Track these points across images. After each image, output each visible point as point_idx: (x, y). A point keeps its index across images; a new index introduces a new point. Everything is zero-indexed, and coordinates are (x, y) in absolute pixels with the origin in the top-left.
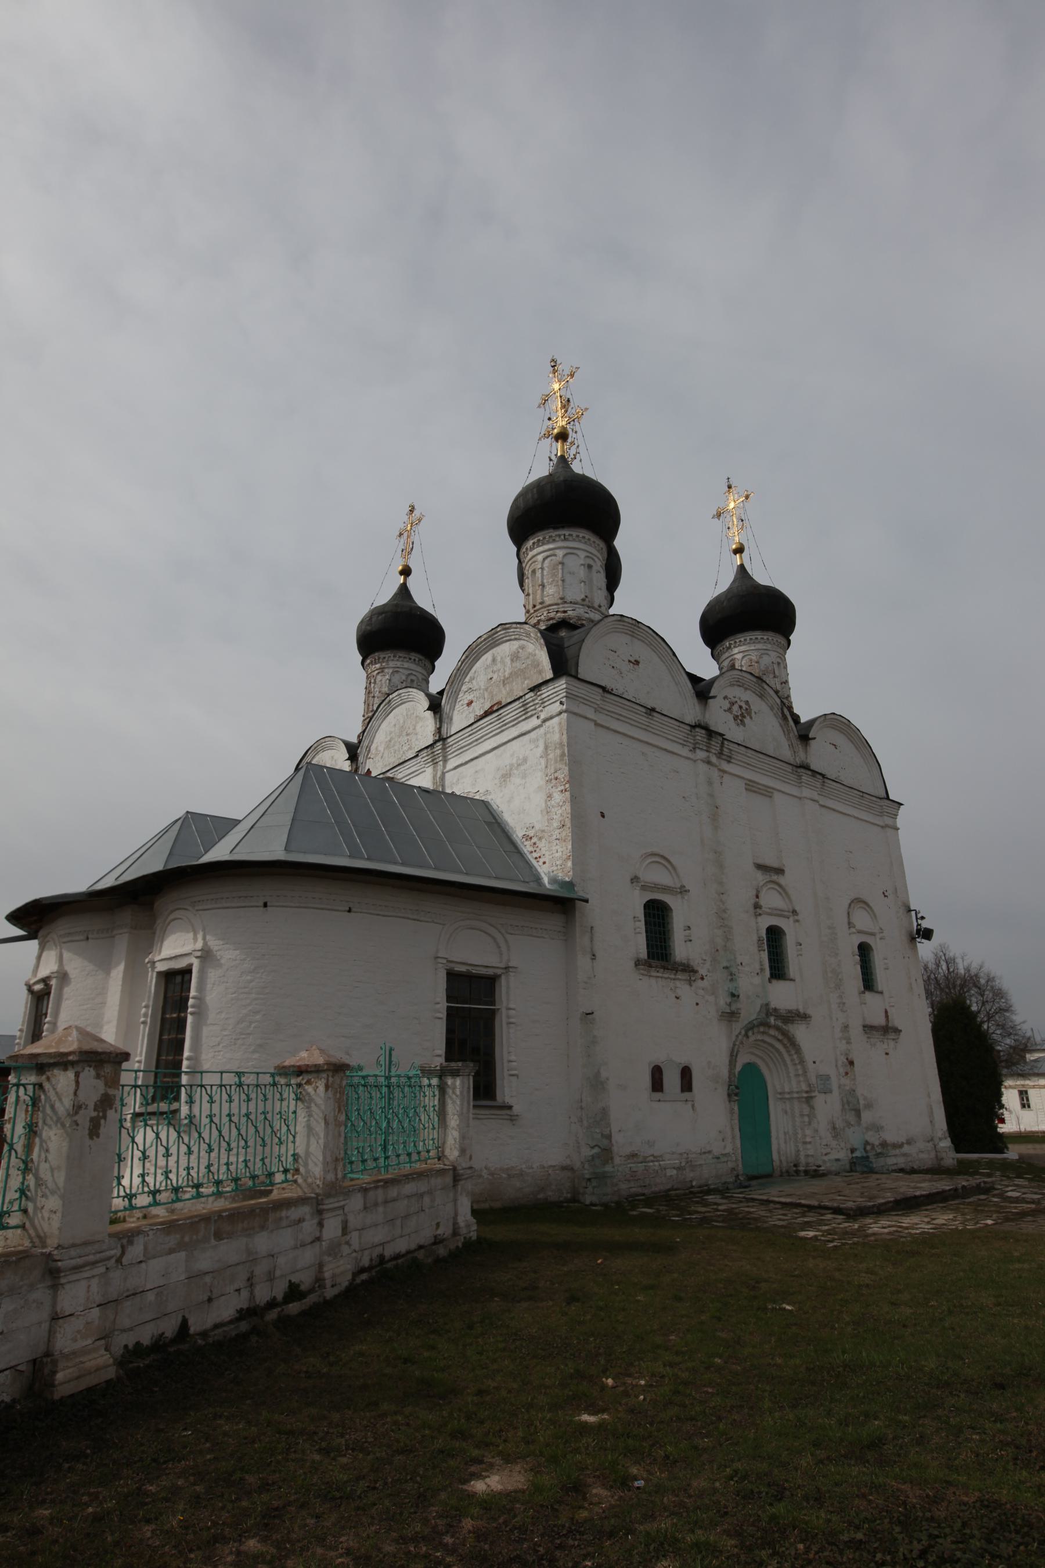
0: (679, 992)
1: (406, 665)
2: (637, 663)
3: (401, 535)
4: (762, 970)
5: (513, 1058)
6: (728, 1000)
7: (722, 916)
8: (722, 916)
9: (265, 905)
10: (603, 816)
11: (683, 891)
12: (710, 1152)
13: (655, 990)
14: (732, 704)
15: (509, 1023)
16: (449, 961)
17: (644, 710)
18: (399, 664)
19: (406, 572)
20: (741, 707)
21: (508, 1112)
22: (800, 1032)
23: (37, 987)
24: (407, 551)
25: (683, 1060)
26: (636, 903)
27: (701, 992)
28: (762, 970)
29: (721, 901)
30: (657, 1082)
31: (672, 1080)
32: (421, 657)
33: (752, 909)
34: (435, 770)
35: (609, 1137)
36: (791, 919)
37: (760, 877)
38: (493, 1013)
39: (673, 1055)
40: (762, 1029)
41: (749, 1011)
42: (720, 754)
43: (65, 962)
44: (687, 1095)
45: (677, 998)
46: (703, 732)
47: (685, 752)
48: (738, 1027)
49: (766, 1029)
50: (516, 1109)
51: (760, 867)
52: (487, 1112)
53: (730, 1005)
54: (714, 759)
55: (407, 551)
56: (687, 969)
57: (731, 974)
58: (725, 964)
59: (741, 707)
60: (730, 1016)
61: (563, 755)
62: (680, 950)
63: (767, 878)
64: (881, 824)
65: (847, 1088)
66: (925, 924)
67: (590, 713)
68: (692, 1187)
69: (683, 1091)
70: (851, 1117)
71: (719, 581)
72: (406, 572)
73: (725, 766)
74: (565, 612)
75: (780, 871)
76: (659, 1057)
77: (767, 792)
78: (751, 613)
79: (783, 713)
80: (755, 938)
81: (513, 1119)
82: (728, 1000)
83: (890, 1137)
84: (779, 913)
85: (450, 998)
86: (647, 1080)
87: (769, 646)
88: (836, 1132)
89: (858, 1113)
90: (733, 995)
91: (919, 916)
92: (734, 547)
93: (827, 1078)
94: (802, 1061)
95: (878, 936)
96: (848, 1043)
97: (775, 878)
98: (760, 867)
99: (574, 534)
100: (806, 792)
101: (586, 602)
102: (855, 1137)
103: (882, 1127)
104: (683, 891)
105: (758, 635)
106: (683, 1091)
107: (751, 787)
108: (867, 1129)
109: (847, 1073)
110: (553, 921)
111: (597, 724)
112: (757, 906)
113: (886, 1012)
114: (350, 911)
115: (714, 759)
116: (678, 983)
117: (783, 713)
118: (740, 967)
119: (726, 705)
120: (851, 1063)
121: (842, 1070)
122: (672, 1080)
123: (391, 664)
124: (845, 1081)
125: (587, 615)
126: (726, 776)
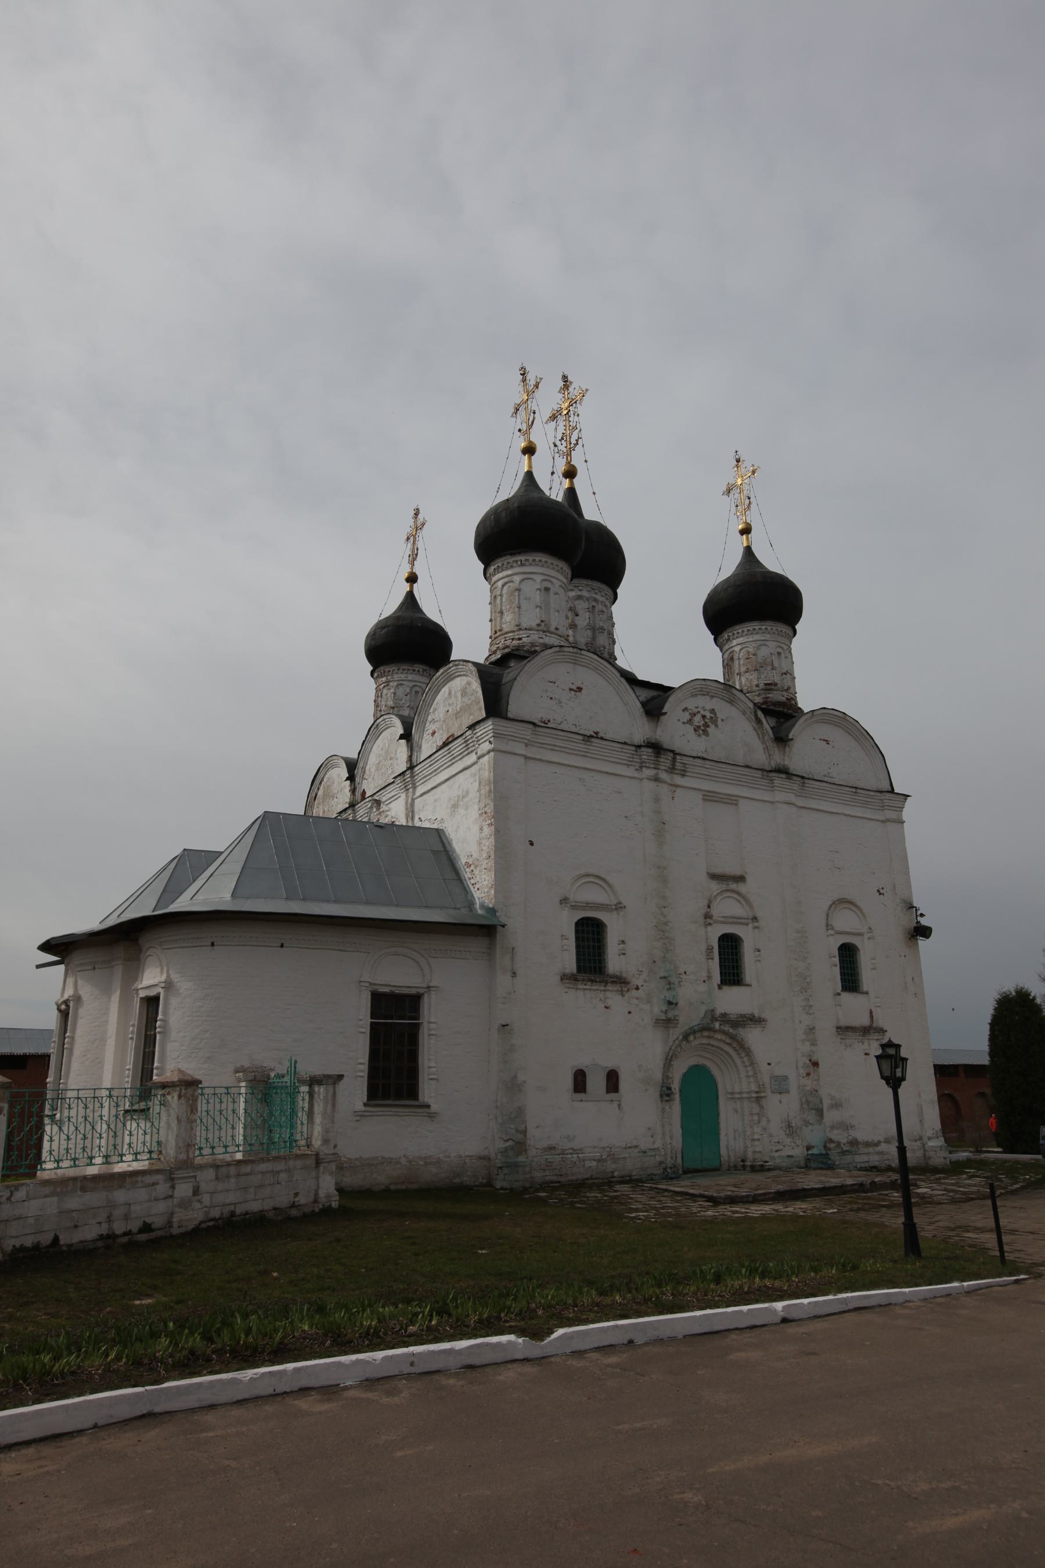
0: (609, 1002)
1: (410, 677)
2: (580, 689)
3: (408, 539)
4: (709, 977)
5: (433, 1064)
6: (664, 1008)
7: (663, 930)
8: (663, 930)
9: (213, 944)
10: (532, 844)
11: (619, 907)
12: (636, 1147)
13: (585, 1003)
15: (429, 1035)
16: (371, 984)
17: (581, 738)
18: (403, 676)
19: (412, 579)
20: (704, 717)
21: (426, 1110)
22: (752, 1036)
23: (63, 1007)
24: (413, 557)
25: (611, 1064)
26: (566, 923)
27: (636, 1001)
28: (709, 977)
29: (662, 914)
31: (596, 1083)
32: (425, 667)
33: (701, 919)
34: (407, 796)
35: (524, 1132)
36: (750, 926)
37: (715, 887)
38: (417, 1026)
39: (597, 1059)
40: (706, 1034)
41: (689, 1017)
42: (672, 770)
43: (79, 987)
44: (613, 1095)
45: (607, 1008)
46: (650, 750)
47: (630, 772)
48: (676, 1033)
49: (712, 1034)
50: (434, 1107)
51: (714, 877)
52: (407, 1110)
53: (666, 1012)
54: (663, 776)
55: (413, 557)
56: (621, 982)
57: (670, 983)
58: (662, 974)
59: (704, 717)
60: (667, 1022)
61: (490, 791)
62: (614, 963)
63: (724, 887)
64: (882, 818)
65: (808, 1088)
66: (924, 921)
67: (520, 749)
68: (613, 1177)
70: (811, 1117)
71: (725, 566)
72: (412, 579)
73: (678, 780)
74: (520, 639)
75: (741, 879)
76: (582, 1061)
77: (732, 801)
78: (755, 602)
79: (756, 716)
80: (704, 947)
81: (432, 1116)
83: (861, 1136)
84: (736, 920)
85: (373, 1015)
86: (569, 1082)
87: (768, 636)
88: (790, 1129)
89: (820, 1113)
90: (670, 1003)
91: (919, 913)
92: (740, 527)
93: (785, 1078)
94: (752, 1064)
95: (866, 936)
96: (814, 1043)
97: (733, 886)
98: (714, 877)
99: (531, 559)
100: (780, 796)
101: (542, 627)
102: (814, 1136)
103: (852, 1127)
104: (619, 907)
105: (755, 625)
106: (608, 1092)
107: (709, 797)
108: (832, 1128)
109: (808, 1074)
111: (526, 758)
112: (707, 916)
113: (871, 1012)
114: (282, 946)
115: (663, 776)
116: (608, 994)
117: (756, 716)
118: (683, 976)
119: (686, 716)
120: (816, 1064)
121: (802, 1071)
122: (596, 1083)
123: (396, 677)
125: (541, 641)
126: (678, 790)
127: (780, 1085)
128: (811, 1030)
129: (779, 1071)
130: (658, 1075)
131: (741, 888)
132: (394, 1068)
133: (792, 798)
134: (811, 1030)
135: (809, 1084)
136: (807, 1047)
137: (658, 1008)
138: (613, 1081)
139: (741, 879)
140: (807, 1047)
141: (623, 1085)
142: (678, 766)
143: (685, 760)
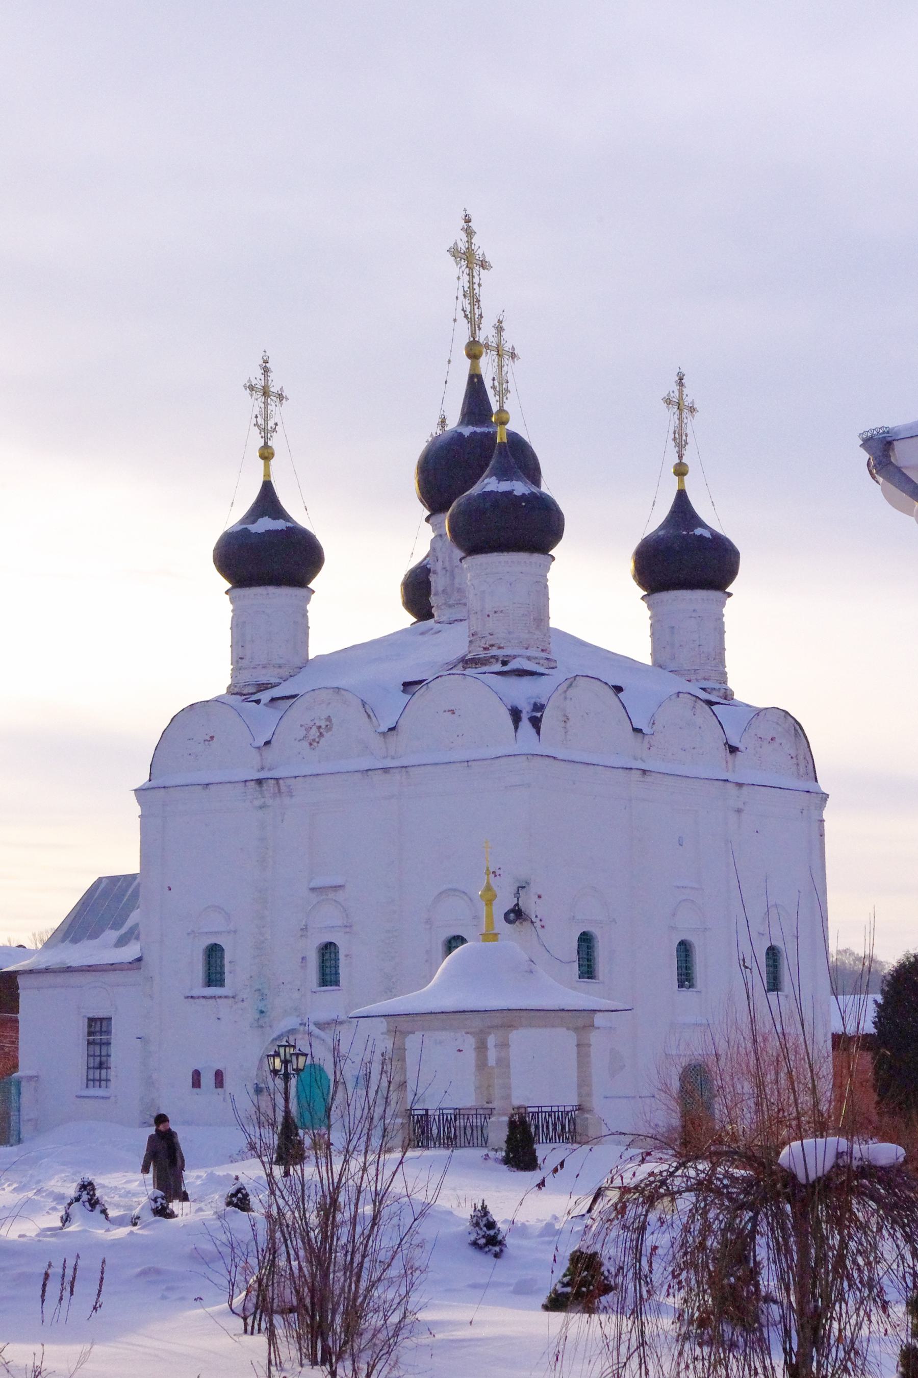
2: (212, 738)
6: (257, 1016)
14: (309, 729)
30: (196, 1080)
31: (208, 1079)
44: (219, 1090)
51: (313, 889)
54: (269, 802)
57: (262, 994)
58: (257, 987)
69: (216, 1087)
82: (257, 1016)
90: (262, 1012)
97: (331, 895)
106: (216, 1087)
115: (269, 802)
122: (208, 1079)
130: (254, 1072)
131: (340, 896)
138: (219, 1077)
142: (283, 788)
143: (288, 782)
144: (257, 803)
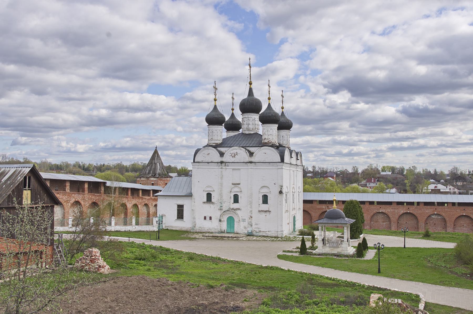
7: (221, 195)
13: (207, 206)
30: (205, 218)
37: (233, 186)
42: (225, 166)
47: (218, 167)
48: (223, 211)
51: (233, 184)
56: (213, 203)
62: (213, 200)
67: (197, 167)
70: (250, 226)
73: (227, 167)
75: (239, 184)
77: (239, 169)
84: (237, 192)
89: (252, 226)
97: (237, 186)
98: (233, 184)
100: (249, 167)
102: (250, 230)
107: (233, 169)
110: (190, 198)
122: (208, 218)
124: (250, 220)
127: (244, 220)
128: (251, 211)
129: (243, 218)
131: (239, 186)
132: (180, 215)
133: (253, 167)
134: (251, 211)
135: (250, 220)
136: (250, 214)
137: (219, 207)
138: (211, 218)
139: (239, 184)
140: (250, 214)
141: (212, 219)
144: (221, 167)
